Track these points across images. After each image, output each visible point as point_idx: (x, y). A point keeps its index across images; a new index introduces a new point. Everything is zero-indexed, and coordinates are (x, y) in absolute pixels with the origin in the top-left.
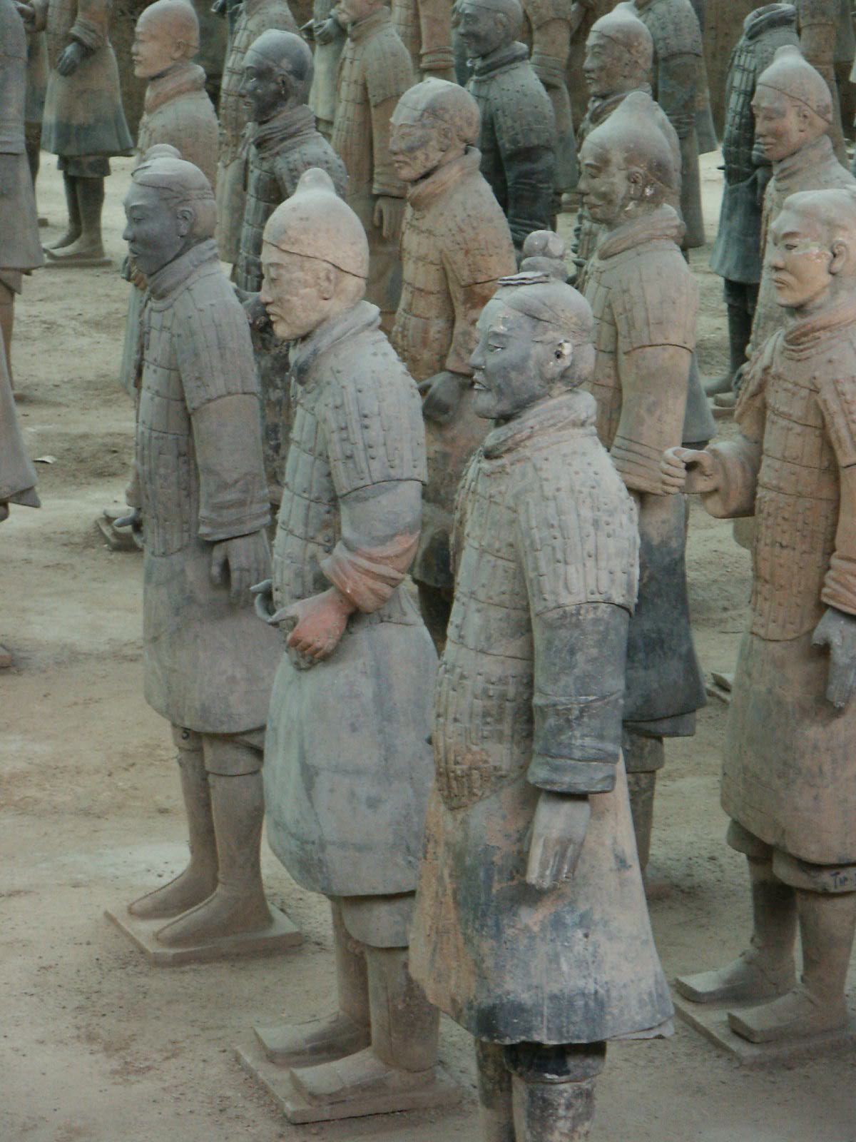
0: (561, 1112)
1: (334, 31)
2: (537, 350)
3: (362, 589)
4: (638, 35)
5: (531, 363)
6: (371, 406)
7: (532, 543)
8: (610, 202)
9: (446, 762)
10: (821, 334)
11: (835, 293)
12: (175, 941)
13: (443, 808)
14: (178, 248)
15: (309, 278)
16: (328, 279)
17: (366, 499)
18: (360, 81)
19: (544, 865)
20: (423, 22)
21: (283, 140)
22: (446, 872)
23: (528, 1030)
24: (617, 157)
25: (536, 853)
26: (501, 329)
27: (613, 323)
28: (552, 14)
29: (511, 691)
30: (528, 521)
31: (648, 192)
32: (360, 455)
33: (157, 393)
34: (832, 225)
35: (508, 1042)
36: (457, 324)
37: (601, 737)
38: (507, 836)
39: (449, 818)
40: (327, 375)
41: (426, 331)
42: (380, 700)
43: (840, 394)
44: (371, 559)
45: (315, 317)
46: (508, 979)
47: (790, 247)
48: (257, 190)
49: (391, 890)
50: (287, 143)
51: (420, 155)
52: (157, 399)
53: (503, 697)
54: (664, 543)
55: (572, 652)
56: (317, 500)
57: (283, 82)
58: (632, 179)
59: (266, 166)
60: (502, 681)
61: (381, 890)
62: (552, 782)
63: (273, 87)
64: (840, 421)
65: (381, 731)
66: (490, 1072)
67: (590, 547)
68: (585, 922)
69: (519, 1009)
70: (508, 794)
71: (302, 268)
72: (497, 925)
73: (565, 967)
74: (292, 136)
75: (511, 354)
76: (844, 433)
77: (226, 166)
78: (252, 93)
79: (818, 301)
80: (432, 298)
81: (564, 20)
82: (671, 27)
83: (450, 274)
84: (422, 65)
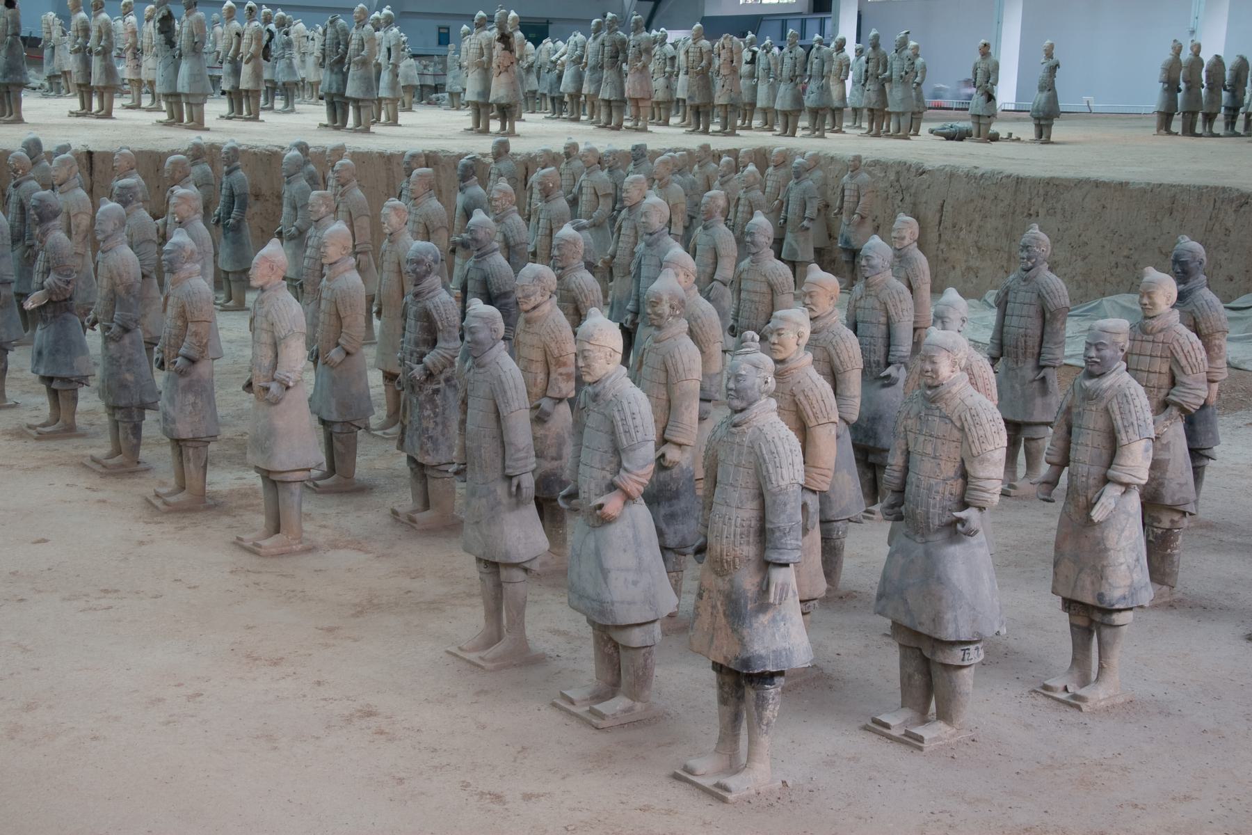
0: (770, 701)
1: (297, 233)
2: (758, 380)
3: (634, 489)
4: (579, 239)
5: (756, 387)
6: (636, 410)
7: (764, 460)
8: (662, 317)
9: (721, 555)
10: (794, 371)
11: (798, 353)
12: (493, 660)
13: (714, 576)
14: (491, 345)
15: (602, 355)
16: (611, 356)
17: (635, 450)
18: (397, 261)
20: (355, 228)
21: (429, 293)
22: (719, 604)
24: (665, 297)
25: (773, 589)
26: (743, 373)
27: (667, 371)
28: (440, 224)
29: (753, 523)
30: (761, 451)
31: (678, 312)
32: (633, 431)
33: (481, 411)
34: (798, 324)
35: (756, 671)
36: (551, 375)
37: (797, 540)
38: (753, 585)
39: (720, 580)
40: (610, 396)
41: (536, 379)
42: (635, 537)
43: (806, 397)
44: (638, 476)
45: (604, 372)
46: (755, 644)
47: (779, 335)
48: (415, 316)
49: (644, 621)
50: (431, 294)
51: (533, 298)
52: (481, 413)
53: (750, 526)
54: (688, 468)
55: (785, 505)
56: (606, 452)
57: (430, 266)
58: (672, 307)
59: (420, 305)
61: (640, 621)
62: (780, 560)
63: (424, 268)
64: (808, 408)
65: (636, 551)
66: (727, 689)
67: (790, 461)
68: (784, 619)
69: (761, 657)
70: (752, 567)
71: (599, 351)
73: (777, 638)
74: (433, 290)
76: (810, 413)
77: (308, 305)
78: (414, 271)
79: (792, 357)
80: (538, 364)
81: (446, 227)
82: (516, 231)
83: (549, 353)
84: (356, 250)
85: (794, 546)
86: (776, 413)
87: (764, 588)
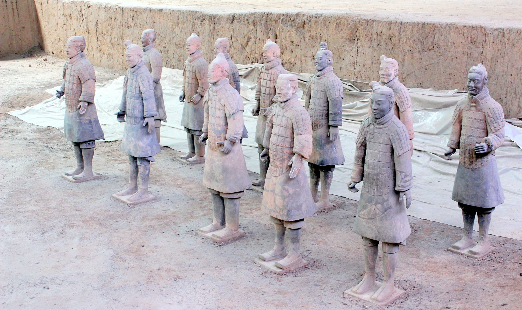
2: (327, 60)
19: (333, 137)
23: (328, 164)
35: (325, 165)
60: (323, 110)
67: (338, 89)
68: (335, 147)
72: (323, 148)
75: (323, 60)
85: (339, 120)
86: (333, 72)
87: (328, 135)
